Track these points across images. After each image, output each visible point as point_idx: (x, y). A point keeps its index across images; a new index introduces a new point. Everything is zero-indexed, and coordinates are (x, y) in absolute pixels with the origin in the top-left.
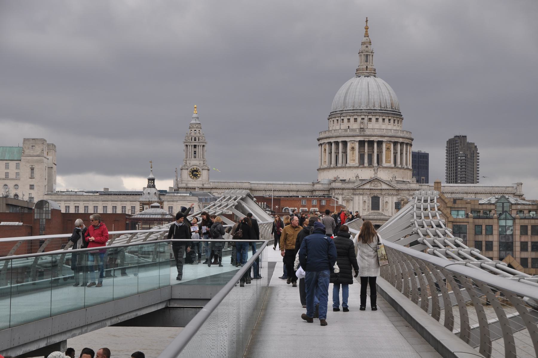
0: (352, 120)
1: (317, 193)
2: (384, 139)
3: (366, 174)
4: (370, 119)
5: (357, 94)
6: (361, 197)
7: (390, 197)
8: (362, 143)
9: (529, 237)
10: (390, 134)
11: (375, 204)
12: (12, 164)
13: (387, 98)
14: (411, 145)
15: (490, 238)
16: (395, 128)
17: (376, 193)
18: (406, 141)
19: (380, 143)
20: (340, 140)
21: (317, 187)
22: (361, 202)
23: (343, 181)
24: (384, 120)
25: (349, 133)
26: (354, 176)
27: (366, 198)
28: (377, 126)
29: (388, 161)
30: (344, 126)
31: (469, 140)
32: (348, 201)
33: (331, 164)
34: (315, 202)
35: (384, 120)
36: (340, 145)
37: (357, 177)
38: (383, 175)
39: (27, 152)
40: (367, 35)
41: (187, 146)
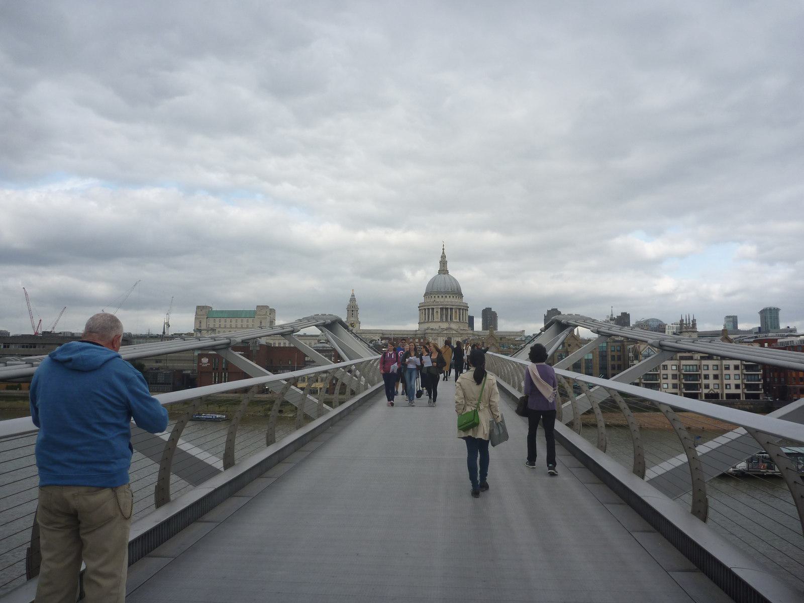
0: (437, 297)
1: (418, 336)
2: (453, 307)
3: (444, 325)
5: (439, 282)
10: (456, 304)
12: (250, 320)
13: (455, 285)
14: (468, 310)
19: (451, 309)
21: (419, 332)
23: (432, 329)
28: (449, 300)
29: (456, 319)
30: (433, 300)
32: (435, 340)
34: (417, 340)
36: (430, 310)
37: (440, 327)
38: (453, 326)
39: (258, 313)
40: (443, 253)
41: (348, 310)
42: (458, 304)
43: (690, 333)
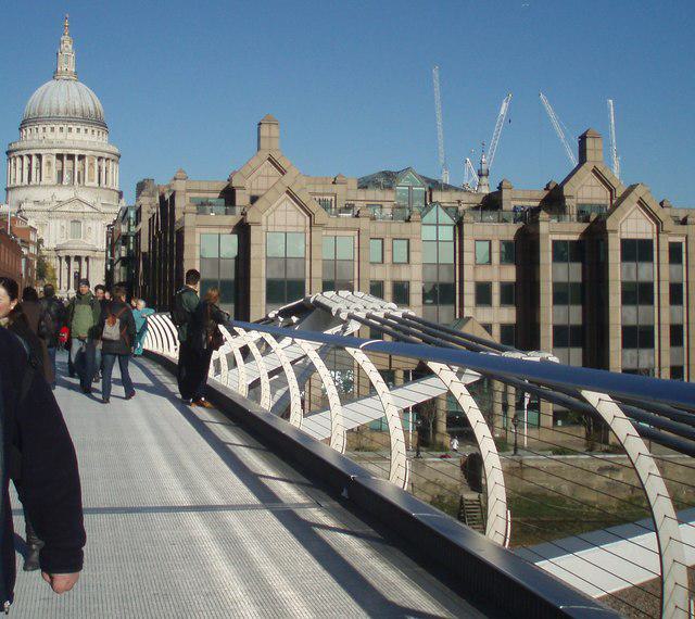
0: (48, 128)
3: (64, 194)
4: (70, 129)
6: (58, 221)
8: (60, 157)
9: (496, 267)
11: (76, 234)
15: (403, 274)
17: (77, 216)
18: (113, 157)
19: (81, 157)
20: (32, 152)
22: (59, 227)
24: (86, 130)
25: (44, 144)
26: (50, 196)
27: (64, 223)
35: (86, 130)
36: (34, 159)
38: (84, 195)
42: (97, 147)
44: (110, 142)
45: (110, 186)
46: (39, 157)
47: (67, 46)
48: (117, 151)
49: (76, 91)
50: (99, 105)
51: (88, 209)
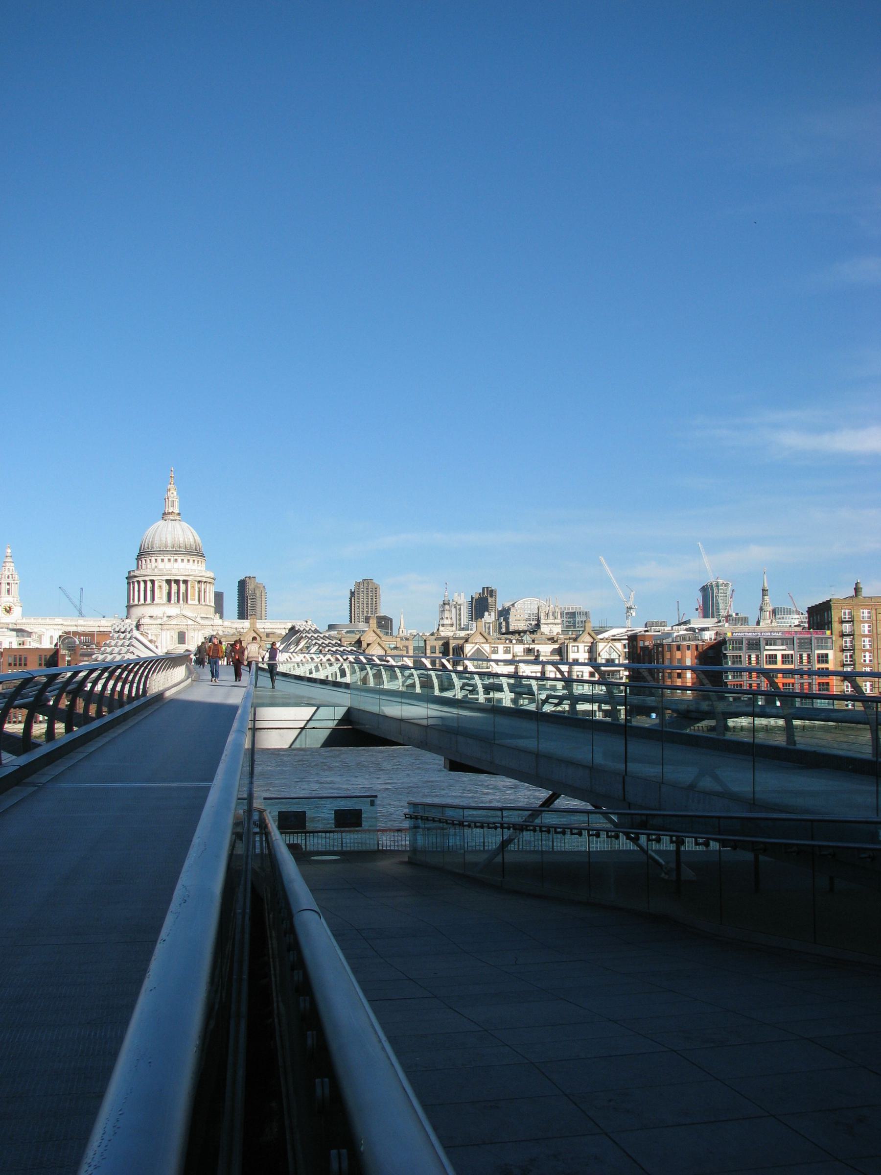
3: (173, 610)
4: (176, 560)
7: (196, 632)
8: (169, 582)
10: (194, 574)
16: (199, 568)
19: (185, 582)
20: (147, 578)
25: (156, 572)
31: (258, 580)
33: (139, 600)
36: (149, 584)
42: (197, 573)
43: (551, 626)
44: (207, 569)
45: (208, 603)
46: (153, 582)
47: (173, 495)
48: (212, 575)
49: (180, 533)
50: (198, 538)
51: (190, 622)
